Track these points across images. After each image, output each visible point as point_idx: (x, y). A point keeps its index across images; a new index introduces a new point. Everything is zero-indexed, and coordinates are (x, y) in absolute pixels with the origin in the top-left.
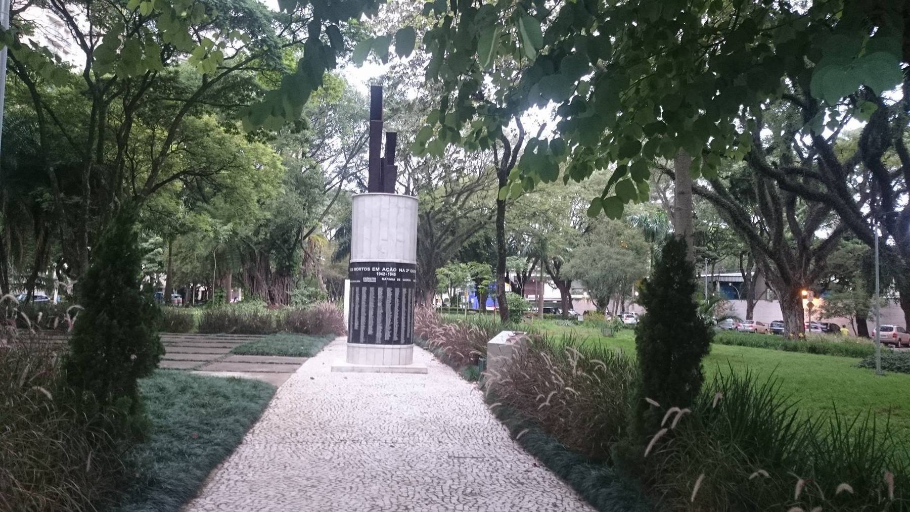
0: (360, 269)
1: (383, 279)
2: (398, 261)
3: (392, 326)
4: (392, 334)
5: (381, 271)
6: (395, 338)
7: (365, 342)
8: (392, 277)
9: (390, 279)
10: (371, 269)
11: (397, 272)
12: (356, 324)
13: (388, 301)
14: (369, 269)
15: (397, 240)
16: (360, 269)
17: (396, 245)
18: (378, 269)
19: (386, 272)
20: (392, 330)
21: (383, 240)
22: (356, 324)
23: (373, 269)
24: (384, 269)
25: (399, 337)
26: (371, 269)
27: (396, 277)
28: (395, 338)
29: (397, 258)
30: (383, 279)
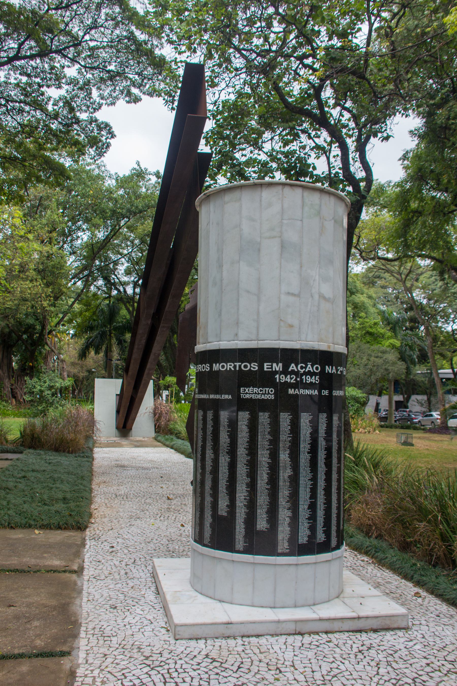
0: (229, 366)
1: (291, 391)
2: (323, 346)
3: (313, 507)
4: (313, 529)
5: (285, 372)
6: (321, 537)
7: (247, 551)
8: (311, 386)
9: (308, 392)
10: (261, 366)
11: (322, 374)
12: (223, 503)
13: (304, 446)
14: (255, 367)
15: (322, 297)
16: (229, 366)
17: (319, 306)
18: (277, 367)
19: (296, 373)
20: (313, 518)
21: (288, 293)
22: (223, 503)
23: (266, 366)
24: (293, 367)
25: (327, 533)
26: (261, 366)
27: (321, 387)
28: (321, 537)
29: (320, 340)
30: (291, 391)
